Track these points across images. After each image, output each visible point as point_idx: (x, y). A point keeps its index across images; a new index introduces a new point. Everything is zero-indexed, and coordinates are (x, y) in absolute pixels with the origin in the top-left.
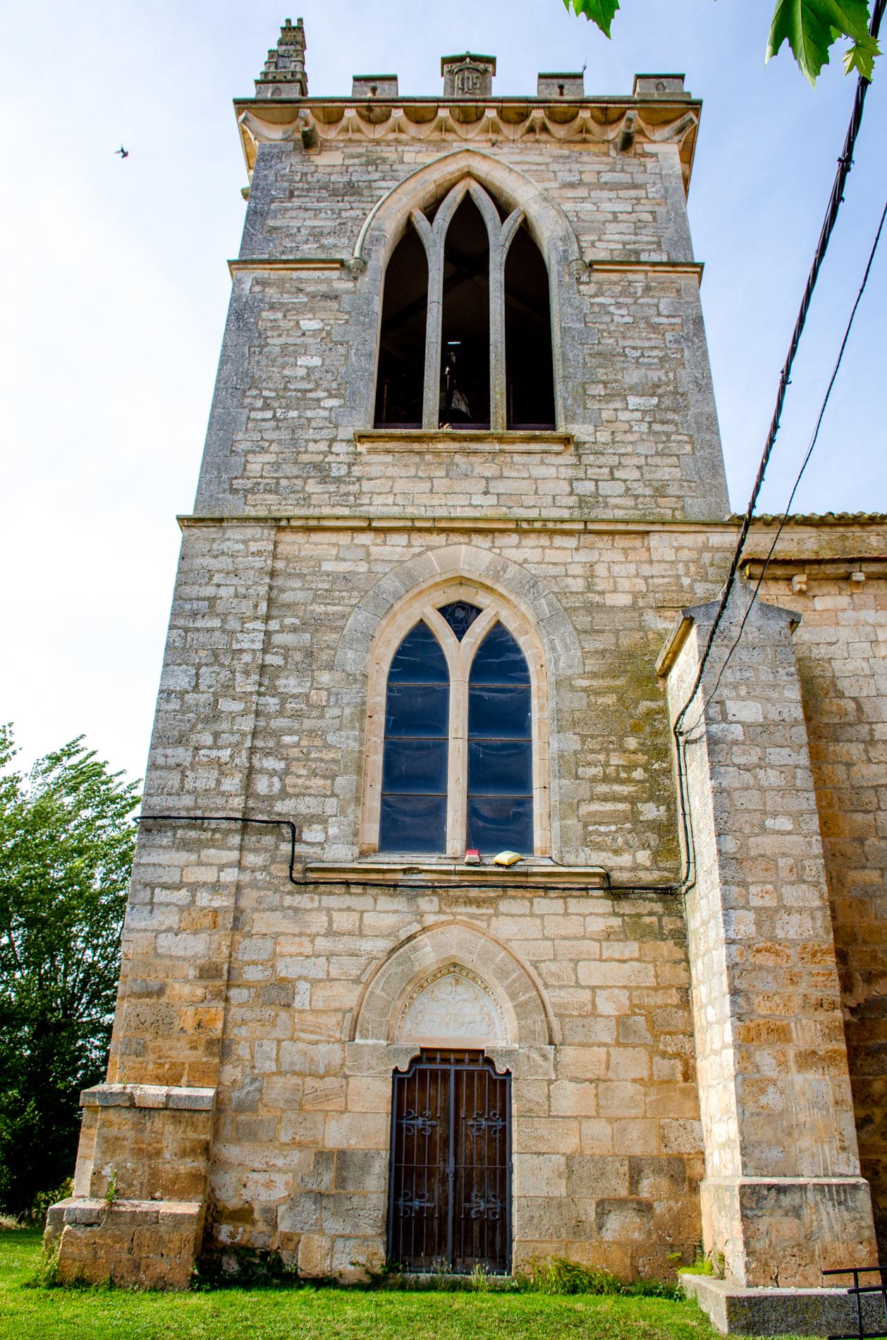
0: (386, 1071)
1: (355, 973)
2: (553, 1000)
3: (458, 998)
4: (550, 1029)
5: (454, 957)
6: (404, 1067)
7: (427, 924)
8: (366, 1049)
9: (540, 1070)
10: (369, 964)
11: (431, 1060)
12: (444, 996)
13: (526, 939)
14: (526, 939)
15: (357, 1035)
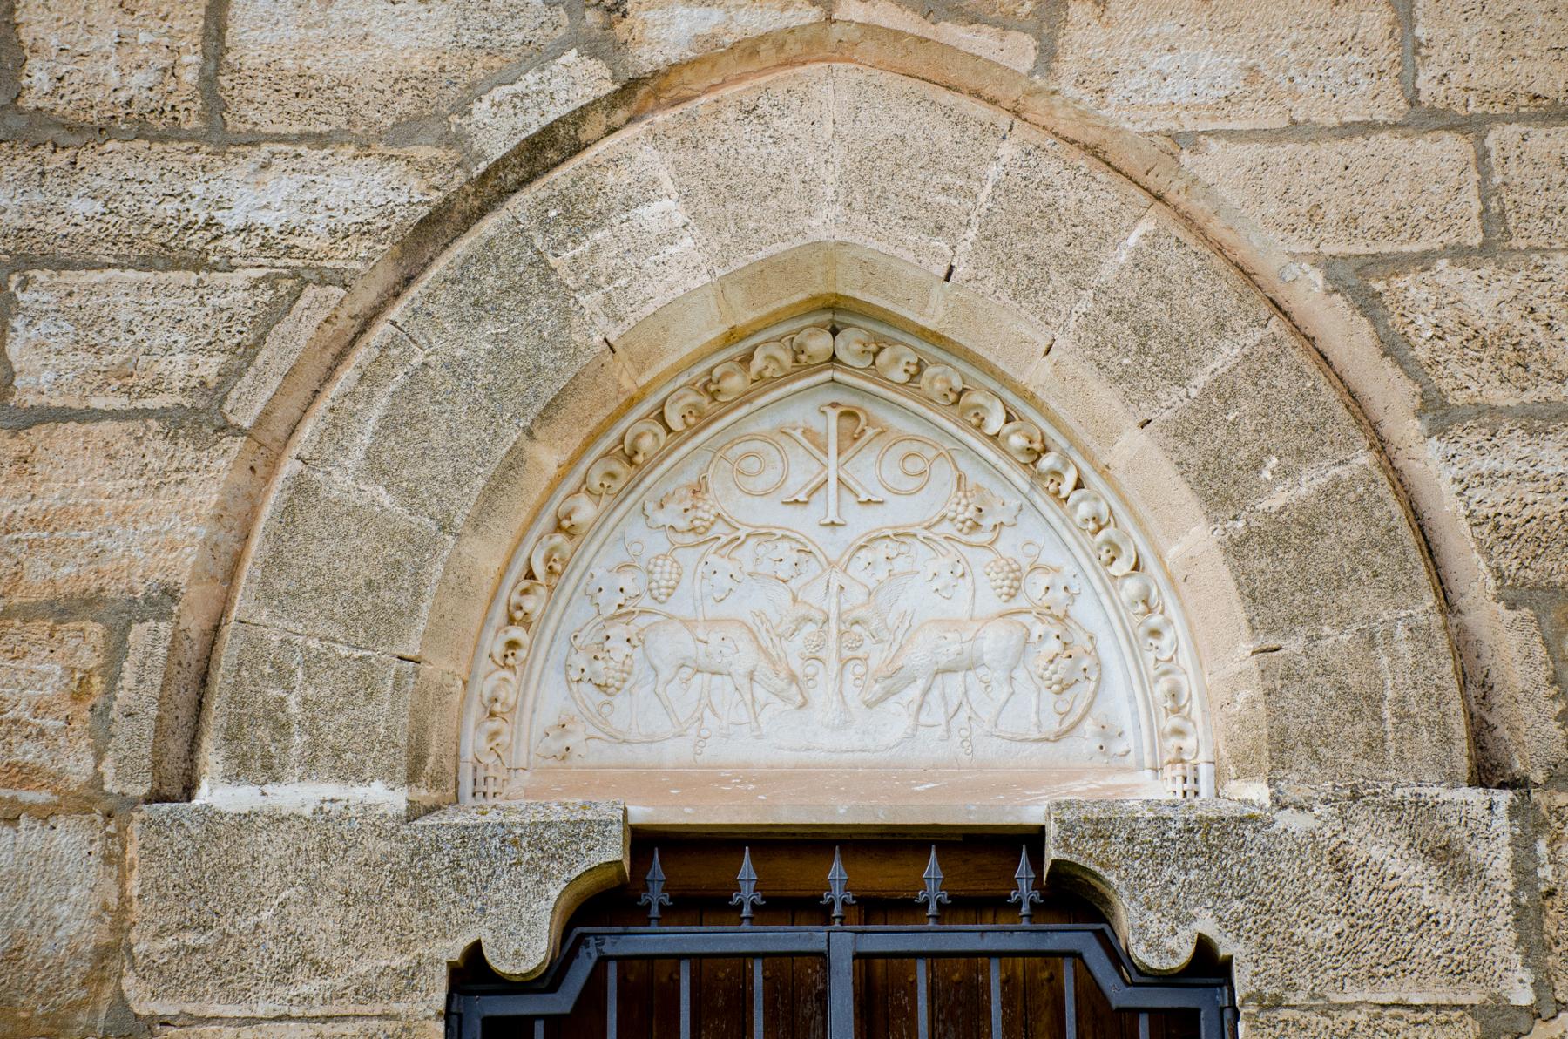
0: (408, 978)
1: (184, 367)
2: (1492, 498)
3: (862, 522)
4: (1477, 687)
5: (829, 252)
6: (524, 947)
7: (646, 58)
8: (273, 847)
9: (1426, 947)
10: (278, 311)
11: (712, 905)
12: (770, 514)
13: (1296, 130)
14: (1296, 130)
15: (212, 757)
